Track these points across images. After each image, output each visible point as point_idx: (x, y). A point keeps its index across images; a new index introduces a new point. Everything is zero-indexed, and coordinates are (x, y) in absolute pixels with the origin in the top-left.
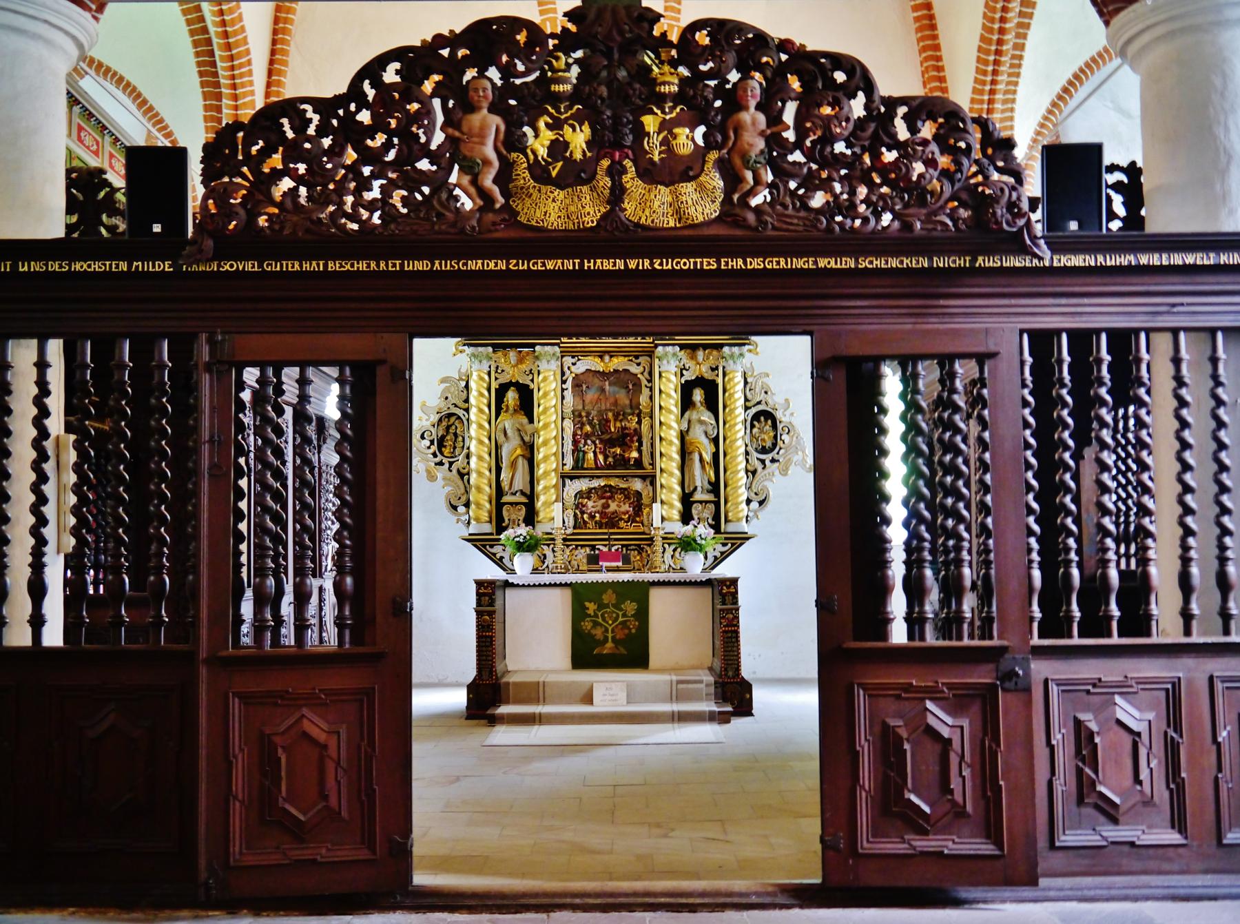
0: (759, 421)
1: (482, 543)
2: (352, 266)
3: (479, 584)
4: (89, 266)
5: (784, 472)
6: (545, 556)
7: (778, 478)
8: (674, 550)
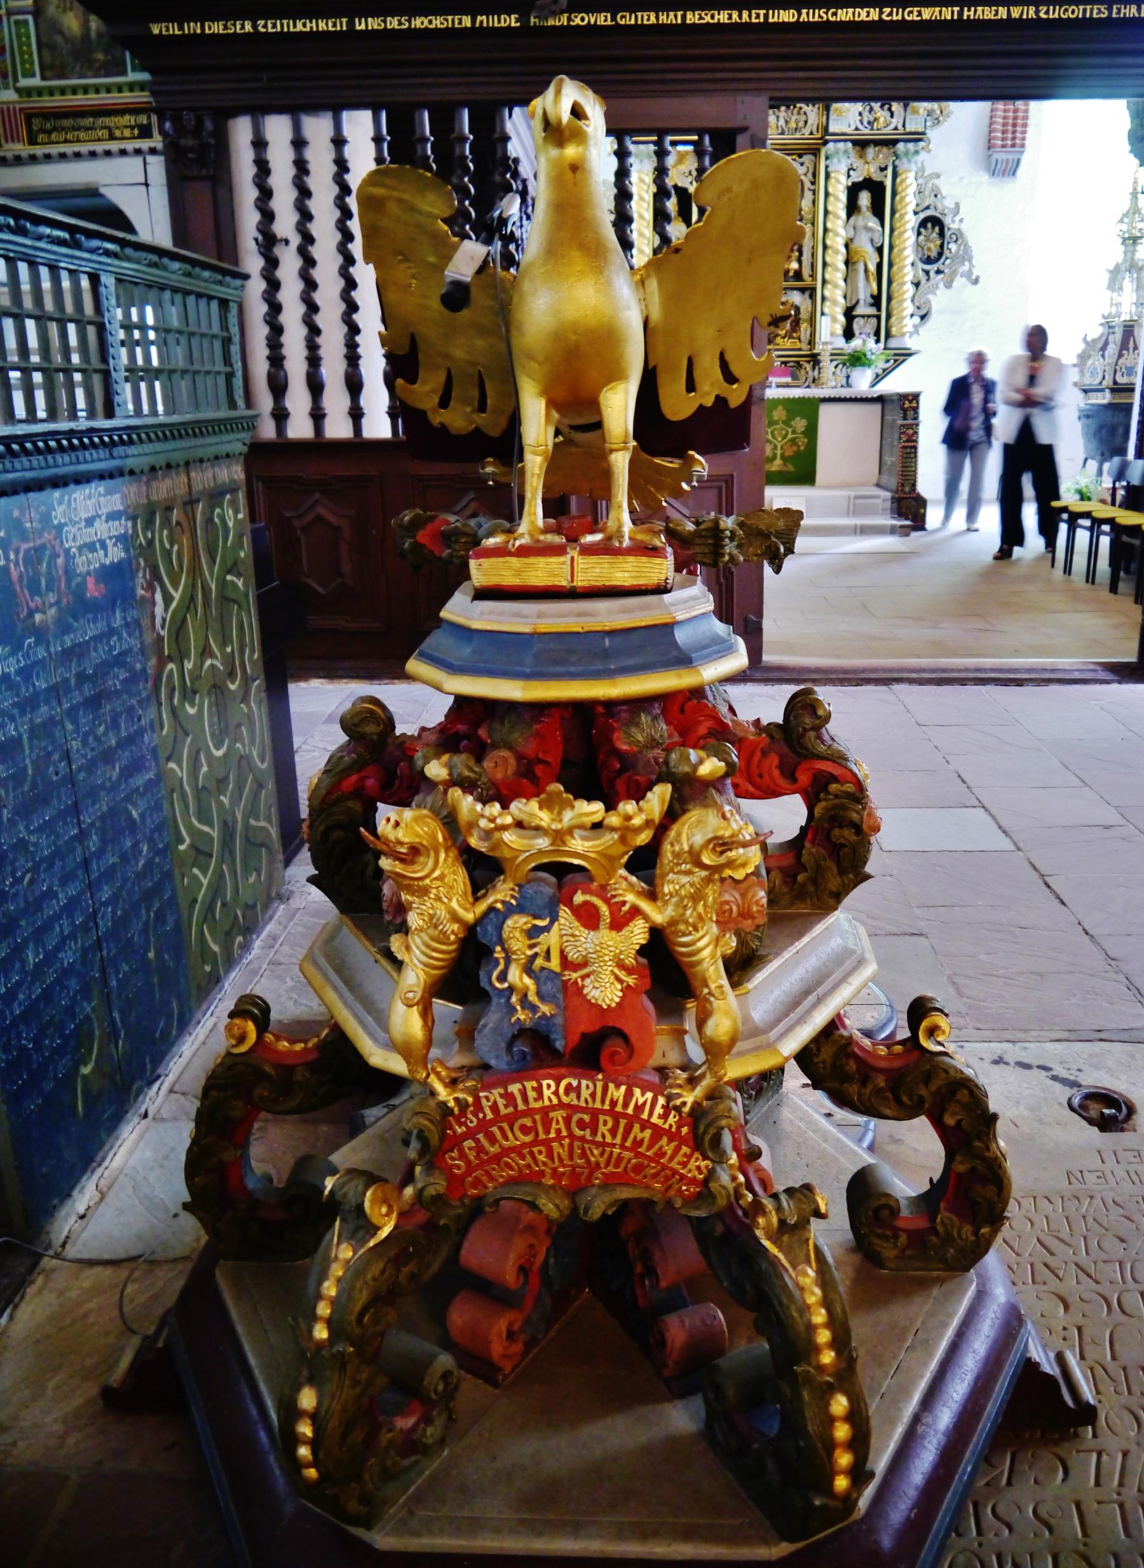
2: (713, 17)
4: (430, 22)
5: (949, 285)
7: (942, 291)
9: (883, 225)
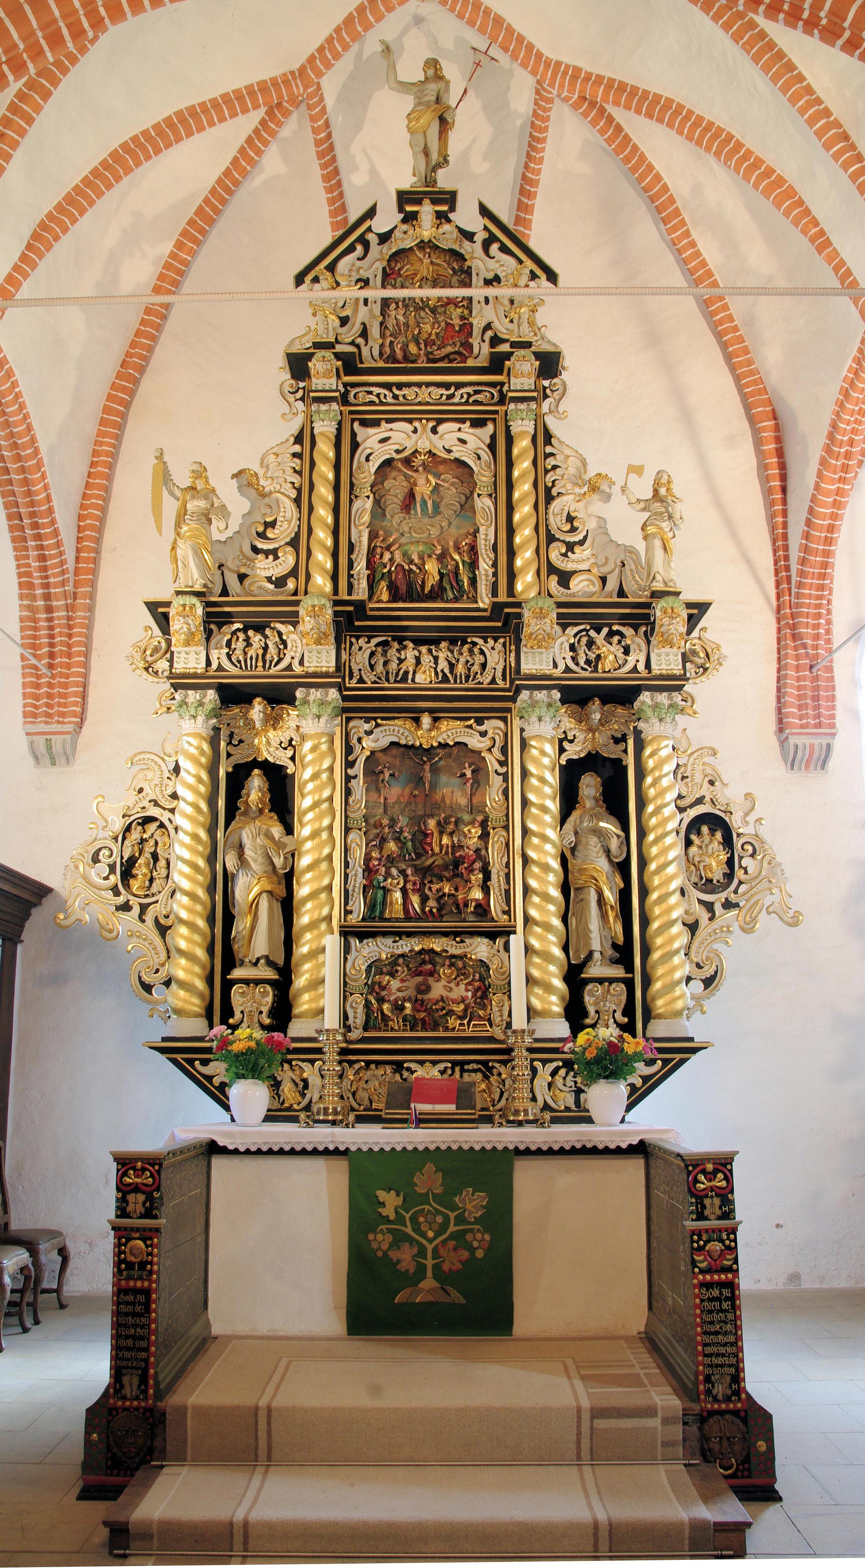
0: (699, 833)
1: (184, 1055)
3: (125, 1163)
6: (305, 1081)
7: (737, 938)
8: (554, 1073)
9: (625, 828)
